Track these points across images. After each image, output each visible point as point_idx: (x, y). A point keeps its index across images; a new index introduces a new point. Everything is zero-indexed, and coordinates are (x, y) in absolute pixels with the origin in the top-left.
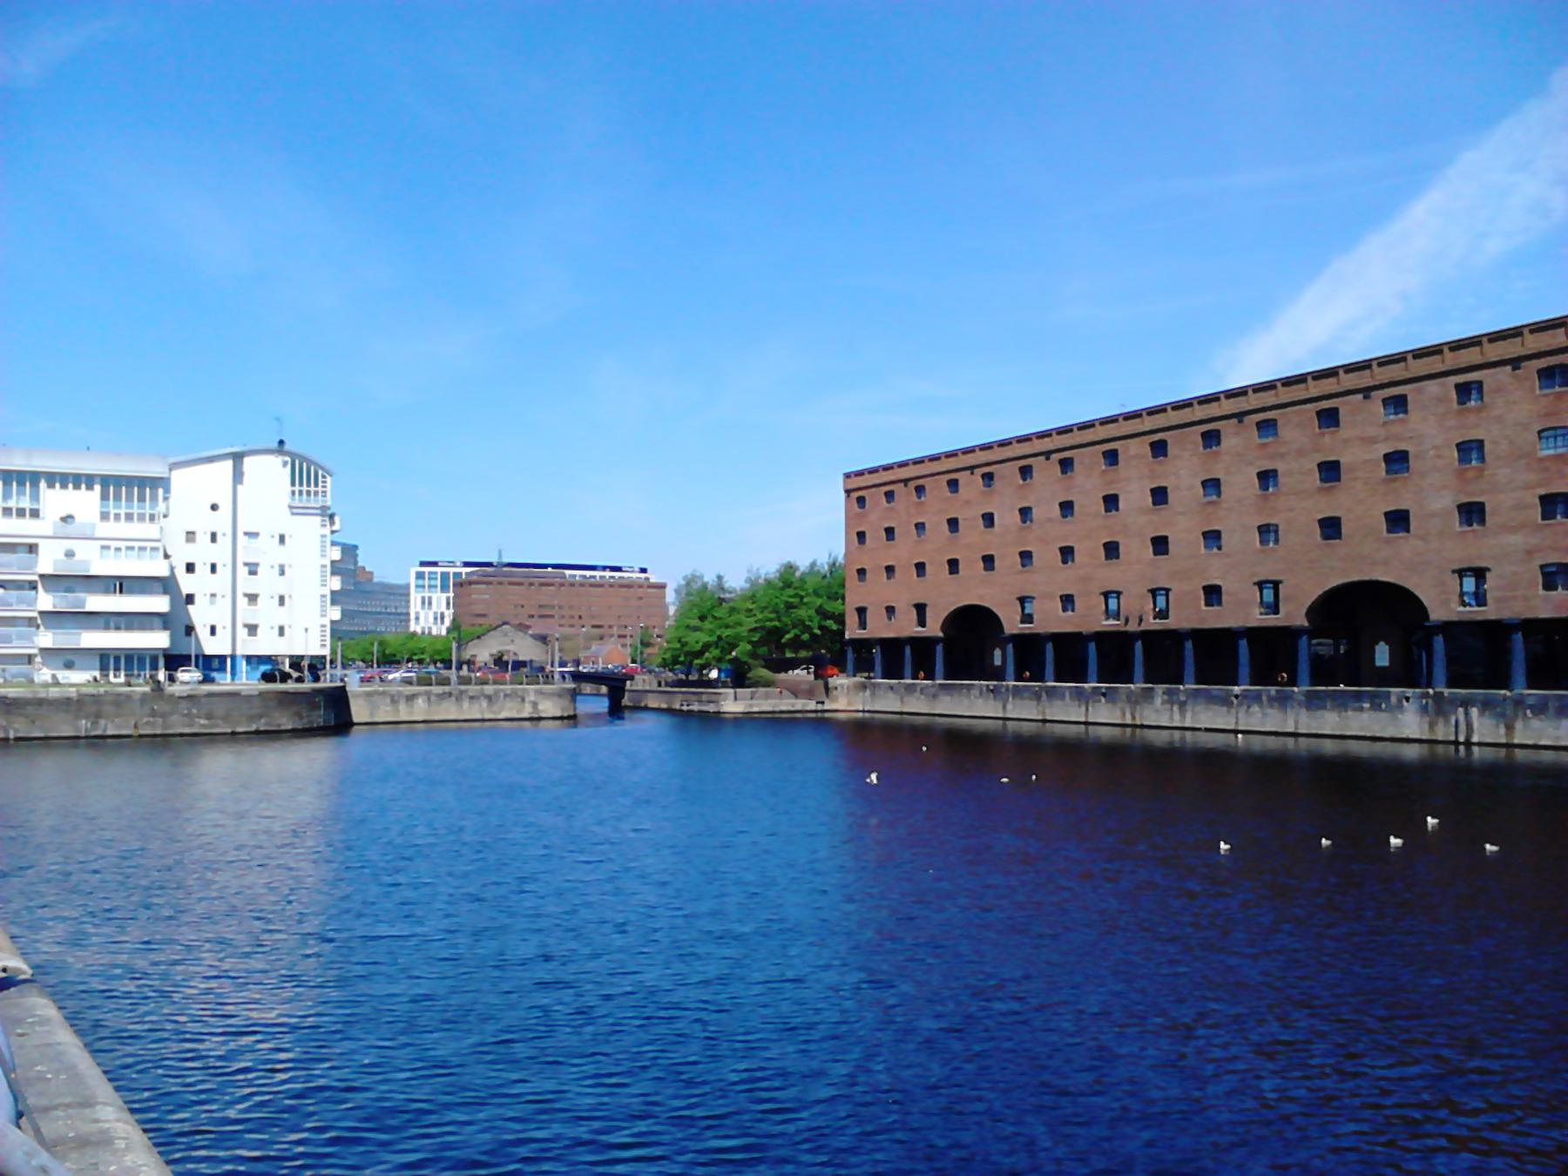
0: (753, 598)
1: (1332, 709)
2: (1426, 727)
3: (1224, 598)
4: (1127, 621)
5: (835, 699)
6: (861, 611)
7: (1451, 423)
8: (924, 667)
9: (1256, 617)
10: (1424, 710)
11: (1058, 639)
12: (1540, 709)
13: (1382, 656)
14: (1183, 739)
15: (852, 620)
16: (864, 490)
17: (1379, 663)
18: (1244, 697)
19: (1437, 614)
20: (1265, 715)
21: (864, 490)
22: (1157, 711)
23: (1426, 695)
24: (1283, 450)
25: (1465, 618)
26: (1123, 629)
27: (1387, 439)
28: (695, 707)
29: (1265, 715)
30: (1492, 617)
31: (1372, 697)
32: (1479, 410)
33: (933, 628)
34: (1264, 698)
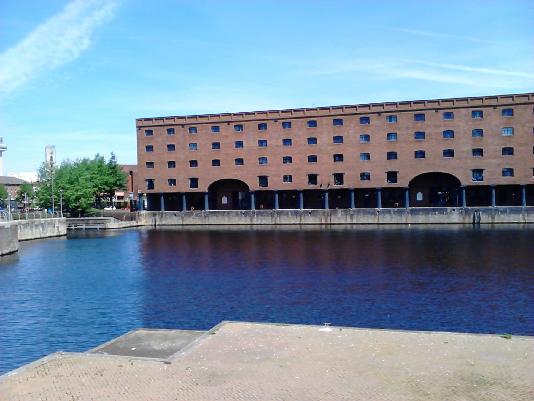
1: (422, 214)
2: (461, 219)
3: (371, 177)
4: (321, 185)
7: (470, 123)
9: (386, 184)
10: (461, 213)
12: (504, 212)
16: (146, 128)
17: (223, 203)
18: (383, 212)
19: (464, 183)
20: (392, 218)
21: (146, 128)
22: (339, 218)
23: (462, 209)
24: (400, 126)
25: (475, 185)
26: (319, 188)
27: (445, 126)
29: (392, 218)
30: (485, 184)
32: (481, 120)
34: (392, 212)
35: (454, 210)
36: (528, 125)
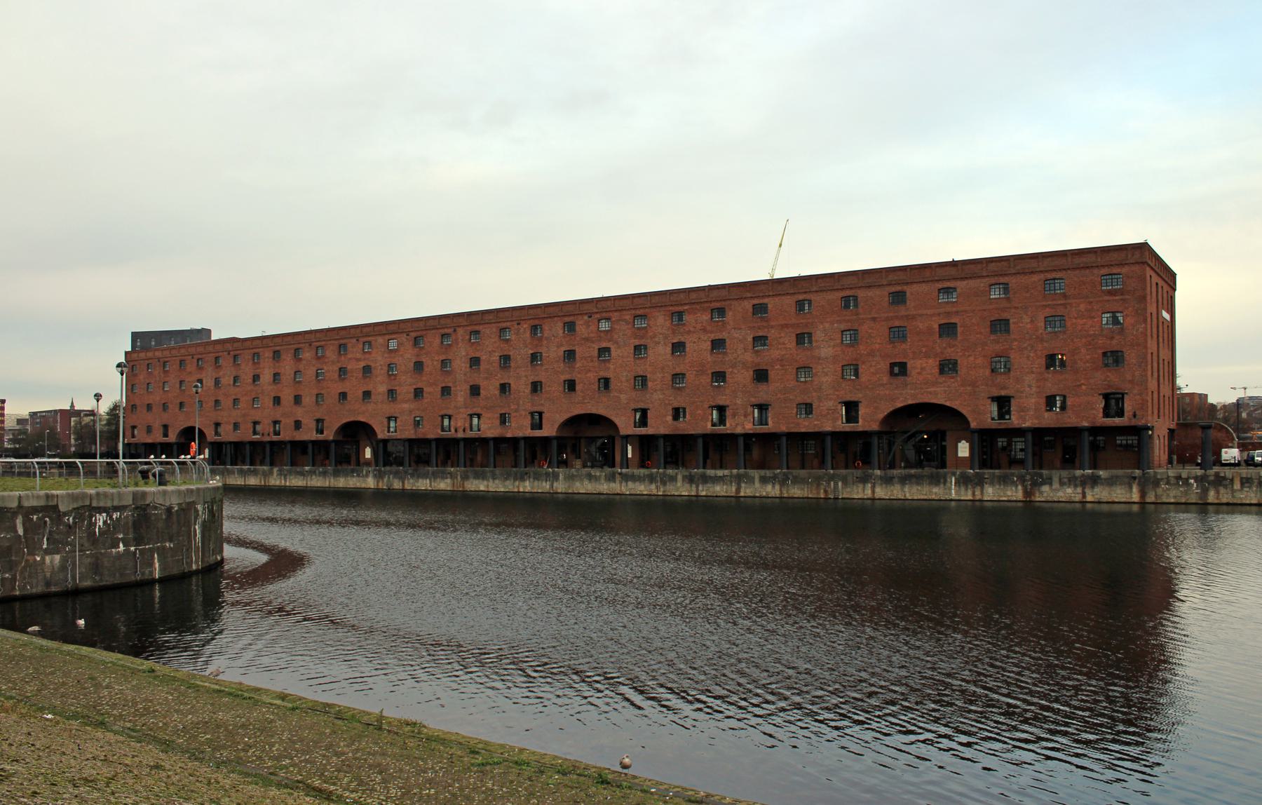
10: (375, 476)
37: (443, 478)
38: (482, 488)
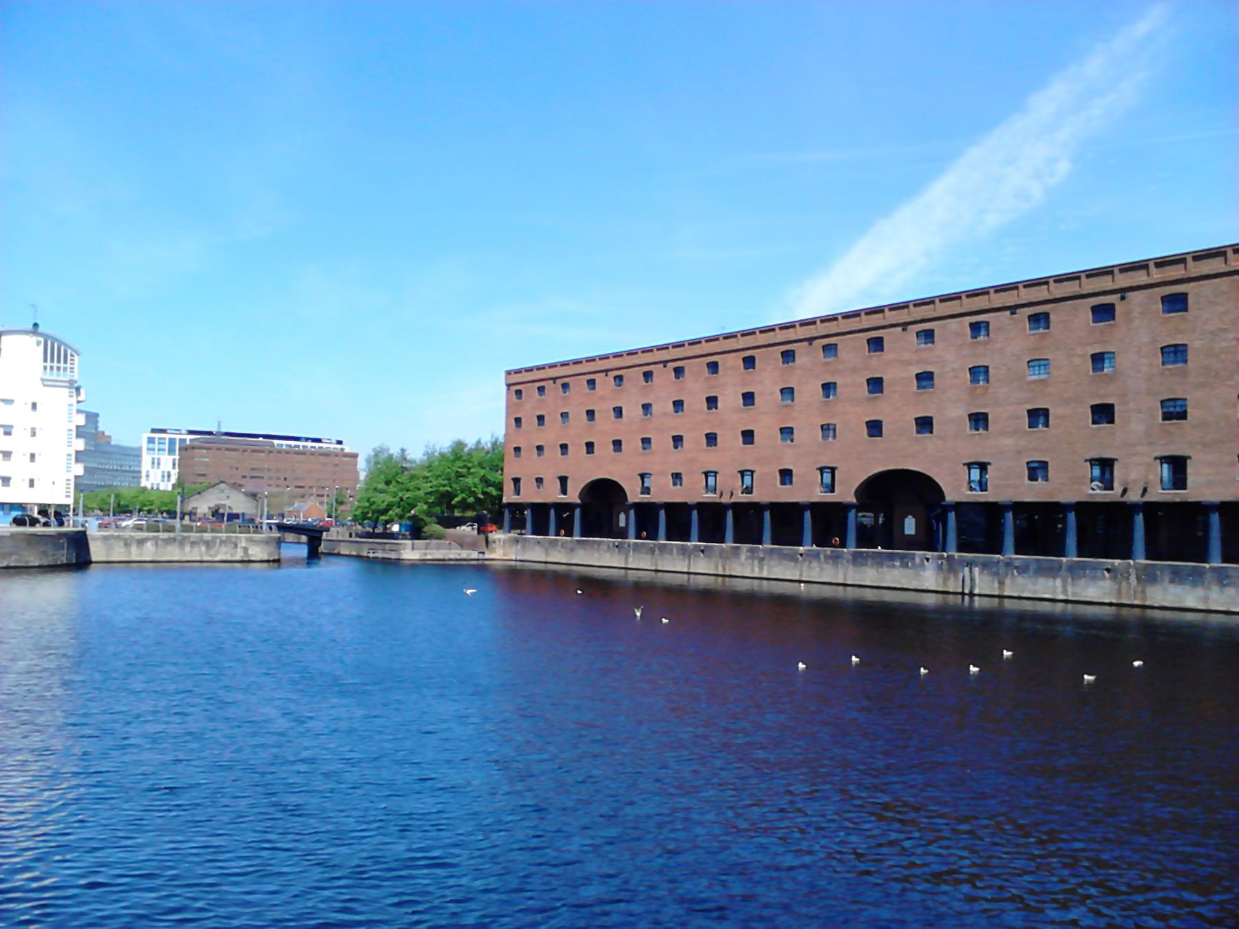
0: (429, 467)
5: (493, 551)
6: (516, 481)
7: (965, 352)
8: (565, 527)
9: (819, 495)
10: (940, 567)
11: (669, 507)
12: (1023, 570)
13: (910, 526)
14: (761, 586)
15: (509, 487)
16: (520, 385)
19: (951, 497)
20: (822, 569)
22: (742, 565)
23: (941, 557)
24: (841, 368)
26: (718, 501)
27: (918, 362)
28: (380, 555)
29: (822, 569)
31: (902, 557)
32: (986, 343)
33: (573, 496)
35: (928, 560)
36: (1079, 351)
37: (1094, 578)
38: (1190, 603)
